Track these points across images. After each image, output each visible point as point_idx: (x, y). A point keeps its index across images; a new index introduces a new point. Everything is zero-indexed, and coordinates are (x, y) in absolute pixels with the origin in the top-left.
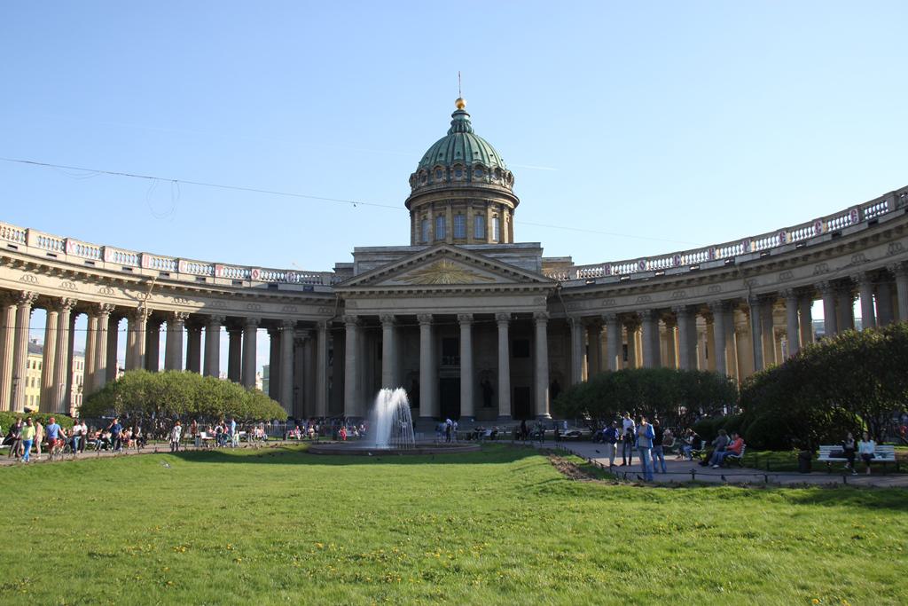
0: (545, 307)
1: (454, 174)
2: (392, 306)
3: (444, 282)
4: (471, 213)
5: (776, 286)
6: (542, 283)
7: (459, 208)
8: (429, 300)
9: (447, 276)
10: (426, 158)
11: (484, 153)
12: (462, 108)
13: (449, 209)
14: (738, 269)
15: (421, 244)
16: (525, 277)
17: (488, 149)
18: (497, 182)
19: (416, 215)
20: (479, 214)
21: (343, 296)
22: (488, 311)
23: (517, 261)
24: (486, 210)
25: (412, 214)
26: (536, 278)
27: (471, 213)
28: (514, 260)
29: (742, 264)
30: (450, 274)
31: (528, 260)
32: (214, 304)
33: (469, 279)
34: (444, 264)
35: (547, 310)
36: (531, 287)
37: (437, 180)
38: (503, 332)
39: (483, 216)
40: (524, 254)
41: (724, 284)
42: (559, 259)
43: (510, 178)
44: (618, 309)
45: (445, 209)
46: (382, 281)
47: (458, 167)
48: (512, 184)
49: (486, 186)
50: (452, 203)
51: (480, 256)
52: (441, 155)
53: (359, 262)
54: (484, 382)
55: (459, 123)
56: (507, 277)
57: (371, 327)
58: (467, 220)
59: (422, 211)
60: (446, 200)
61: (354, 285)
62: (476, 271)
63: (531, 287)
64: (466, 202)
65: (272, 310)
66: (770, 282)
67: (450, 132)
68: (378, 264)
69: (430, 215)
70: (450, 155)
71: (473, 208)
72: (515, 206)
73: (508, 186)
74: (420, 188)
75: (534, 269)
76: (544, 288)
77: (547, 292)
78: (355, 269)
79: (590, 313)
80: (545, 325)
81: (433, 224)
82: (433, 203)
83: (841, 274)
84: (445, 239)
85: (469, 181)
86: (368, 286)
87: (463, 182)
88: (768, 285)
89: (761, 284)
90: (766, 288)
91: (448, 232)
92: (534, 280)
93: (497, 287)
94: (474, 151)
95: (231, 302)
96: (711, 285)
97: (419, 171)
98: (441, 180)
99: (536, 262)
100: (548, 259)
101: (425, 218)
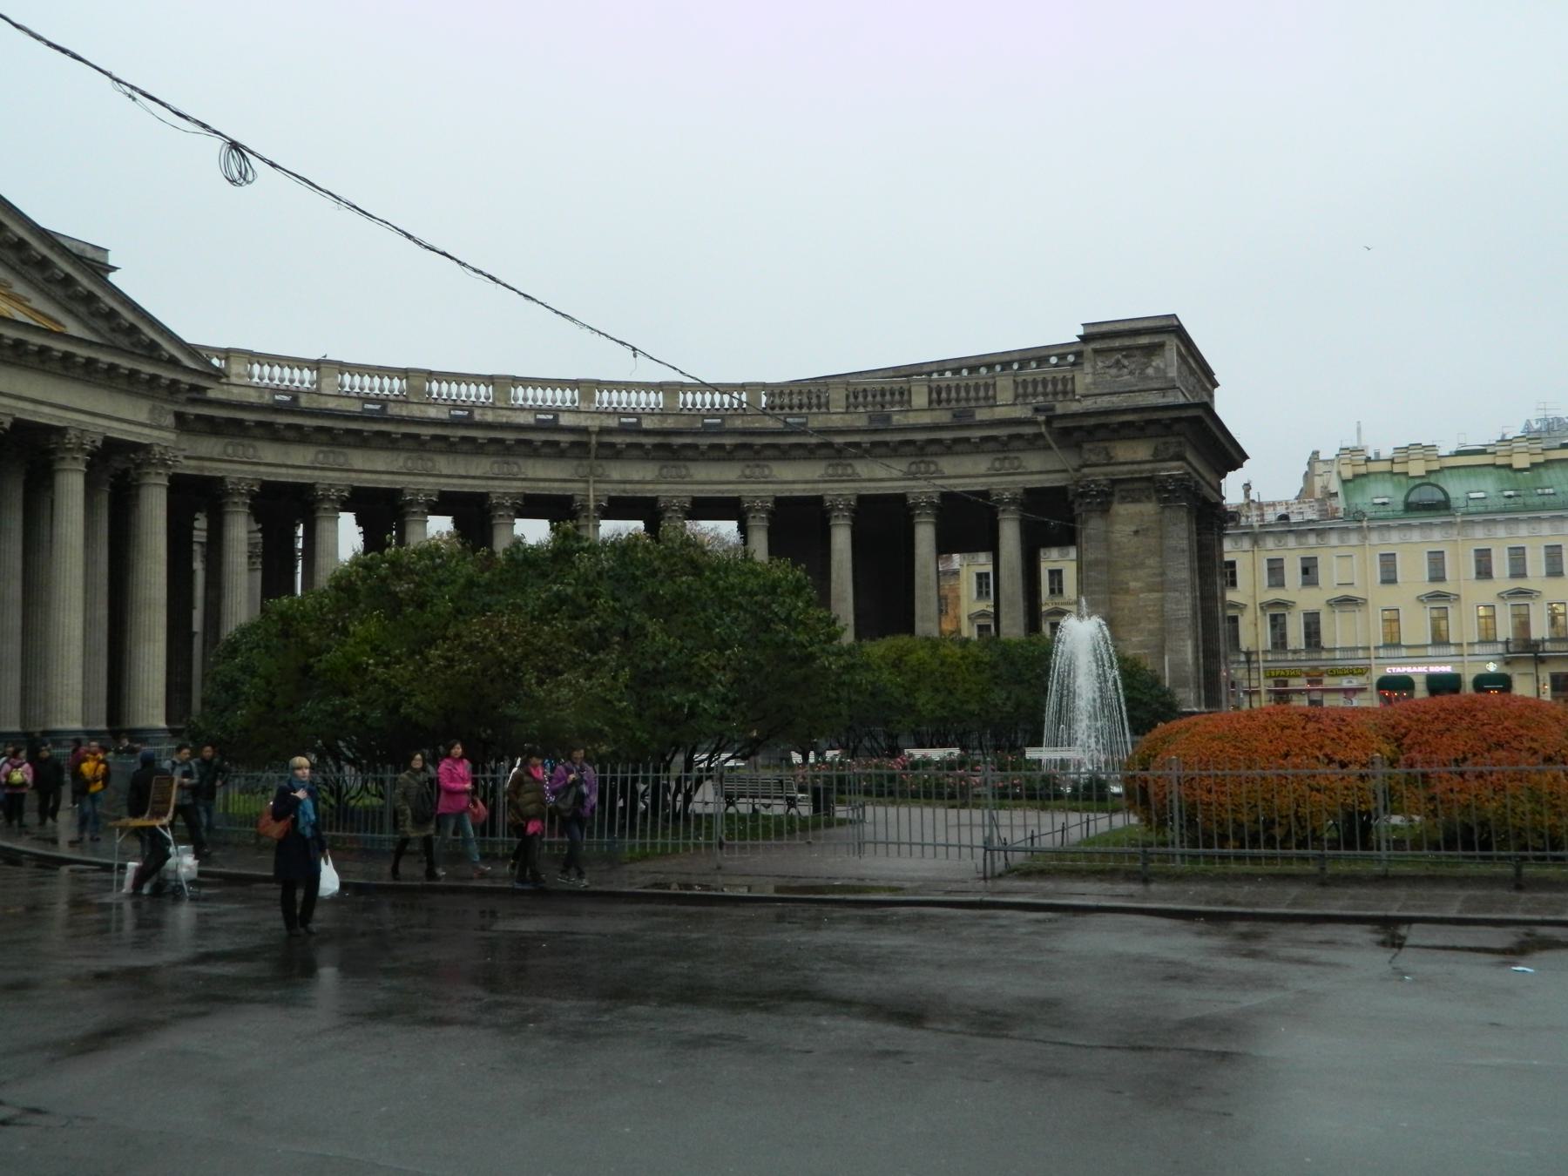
5: (650, 487)
6: (187, 369)
14: (594, 439)
16: (153, 345)
22: (46, 415)
29: (604, 431)
36: (167, 374)
44: (262, 469)
56: (94, 330)
62: (20, 288)
63: (167, 374)
66: (636, 477)
83: (799, 490)
88: (631, 482)
89: (616, 476)
90: (628, 487)
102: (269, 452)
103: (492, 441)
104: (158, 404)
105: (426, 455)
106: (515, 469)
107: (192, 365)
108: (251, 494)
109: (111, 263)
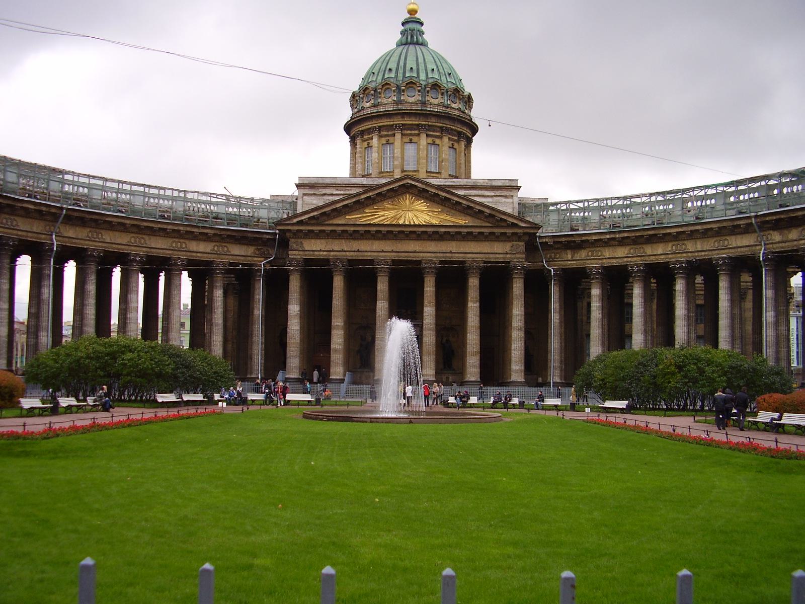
0: (523, 256)
1: (405, 93)
2: (345, 249)
3: (407, 223)
4: (423, 140)
5: (795, 243)
7: (411, 135)
8: (388, 242)
9: (410, 215)
10: (371, 73)
11: (441, 71)
12: (417, 16)
13: (398, 135)
14: (753, 220)
15: (363, 176)
17: (444, 65)
18: (454, 106)
19: (358, 141)
20: (434, 144)
21: (288, 234)
22: (457, 257)
23: (490, 200)
24: (440, 137)
25: (353, 140)
26: (515, 221)
27: (423, 140)
28: (489, 200)
30: (418, 213)
31: (503, 200)
32: (133, 240)
33: (435, 222)
34: (407, 200)
35: (527, 259)
36: (509, 231)
37: (385, 101)
38: (474, 283)
39: (439, 145)
40: (498, 193)
41: (733, 238)
42: (534, 199)
43: (468, 101)
45: (394, 135)
46: (334, 217)
47: (411, 84)
48: (471, 108)
49: (441, 109)
50: (403, 127)
51: (448, 192)
52: (390, 70)
53: (303, 194)
54: (444, 341)
55: (412, 33)
57: (317, 276)
58: (418, 149)
59: (365, 137)
60: (396, 124)
61: (301, 223)
63: (509, 231)
64: (418, 126)
65: (201, 249)
67: (398, 45)
68: (326, 197)
69: (375, 141)
70: (401, 71)
71: (427, 136)
72: (474, 135)
73: (466, 111)
74: (363, 109)
75: (509, 211)
76: (525, 234)
77: (527, 238)
78: (299, 202)
79: (573, 264)
80: (522, 281)
81: (377, 152)
82: (380, 127)
84: (393, 172)
85: (424, 103)
86: (318, 225)
87: (416, 103)
91: (396, 163)
92: (513, 223)
93: (469, 230)
94: (430, 67)
95: (152, 237)
96: (718, 238)
97: (364, 90)
98: (390, 100)
99: (513, 203)
100: (520, 199)
101: (369, 146)
102: (607, 253)
103: (707, 230)
104: (515, 243)
105: (681, 242)
106: (726, 243)
107: (523, 225)
108: (598, 273)
109: (519, 185)
